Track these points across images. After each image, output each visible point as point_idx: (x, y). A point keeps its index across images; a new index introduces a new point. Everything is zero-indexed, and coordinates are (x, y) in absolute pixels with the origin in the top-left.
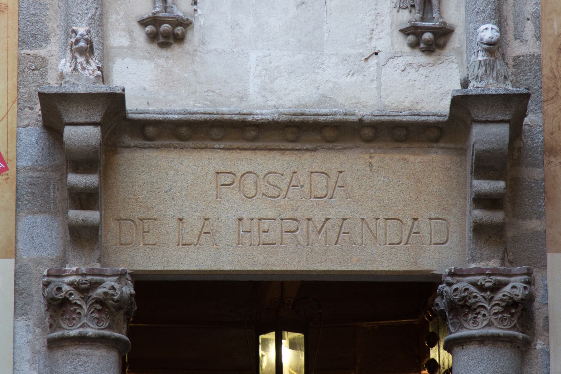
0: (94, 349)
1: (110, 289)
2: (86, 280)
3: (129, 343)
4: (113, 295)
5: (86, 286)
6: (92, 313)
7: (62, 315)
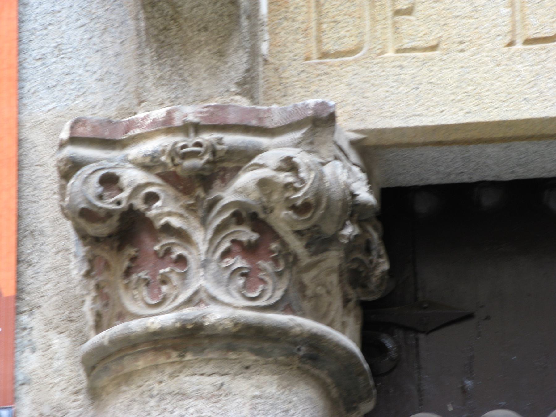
0: (236, 375)
1: (279, 169)
2: (198, 144)
3: (351, 354)
4: (288, 186)
5: (198, 162)
6: (226, 254)
7: (128, 273)
